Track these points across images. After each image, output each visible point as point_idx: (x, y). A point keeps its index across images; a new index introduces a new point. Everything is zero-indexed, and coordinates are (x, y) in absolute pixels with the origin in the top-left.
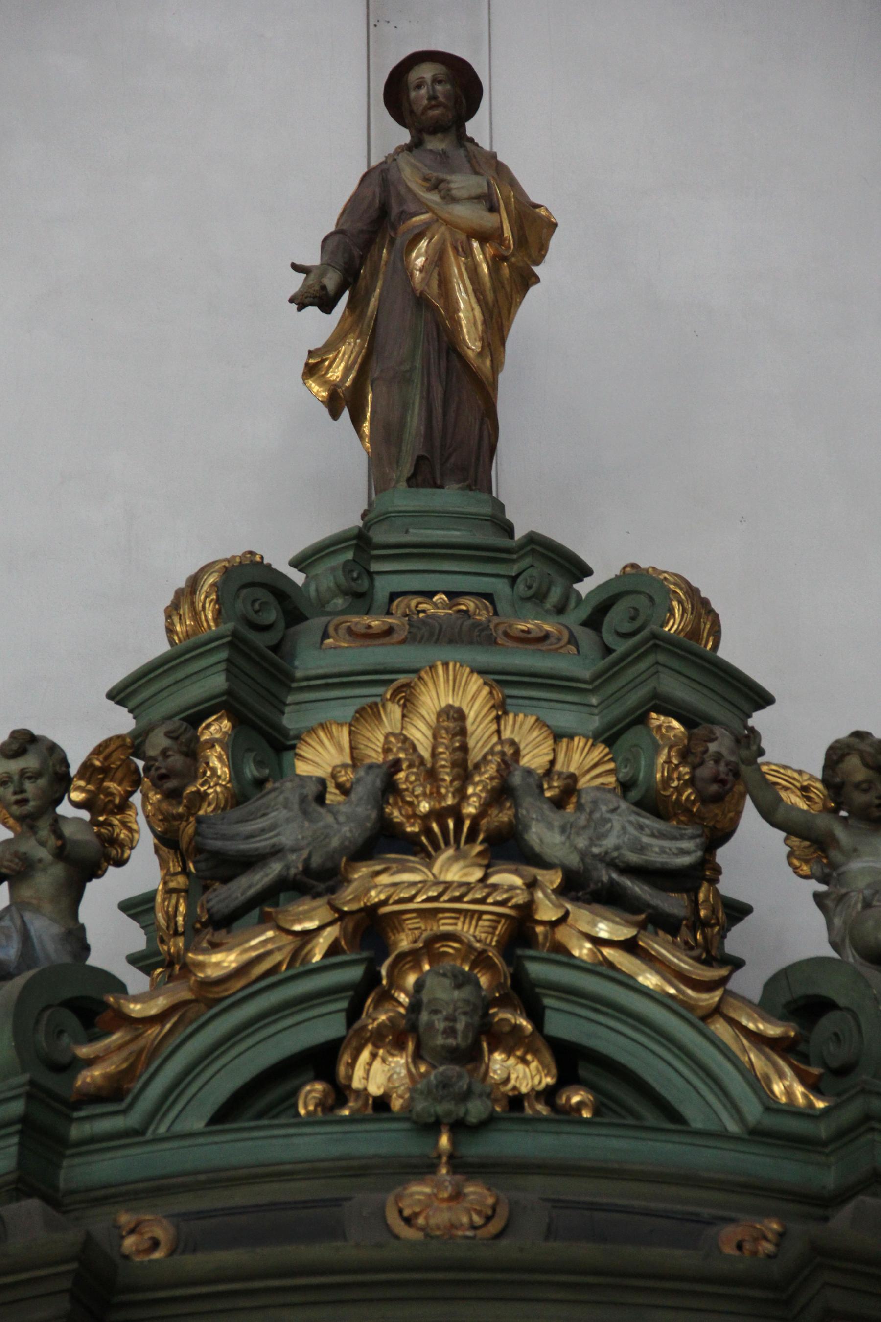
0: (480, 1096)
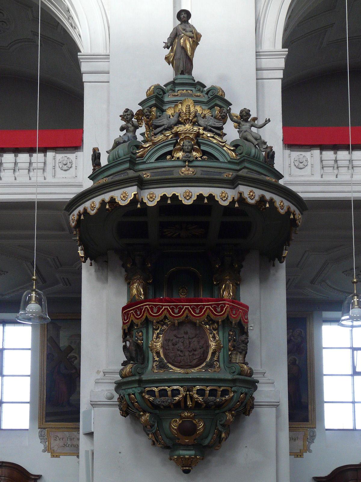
0: (192, 157)
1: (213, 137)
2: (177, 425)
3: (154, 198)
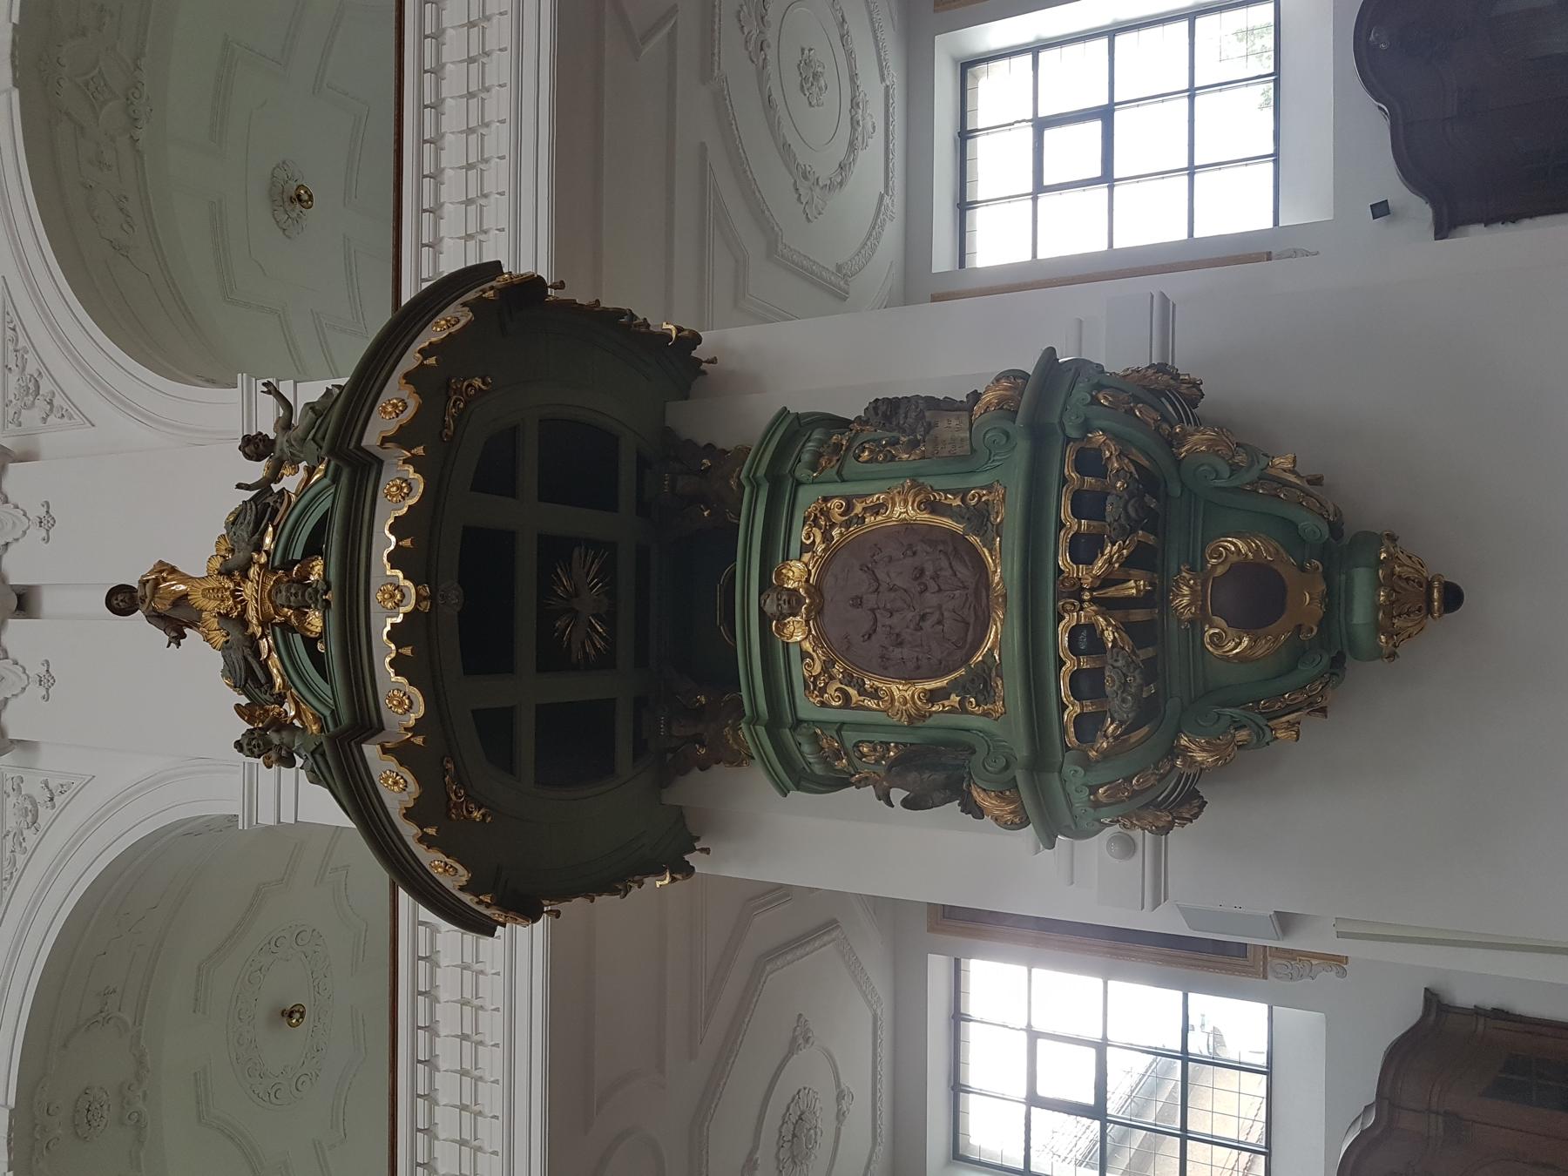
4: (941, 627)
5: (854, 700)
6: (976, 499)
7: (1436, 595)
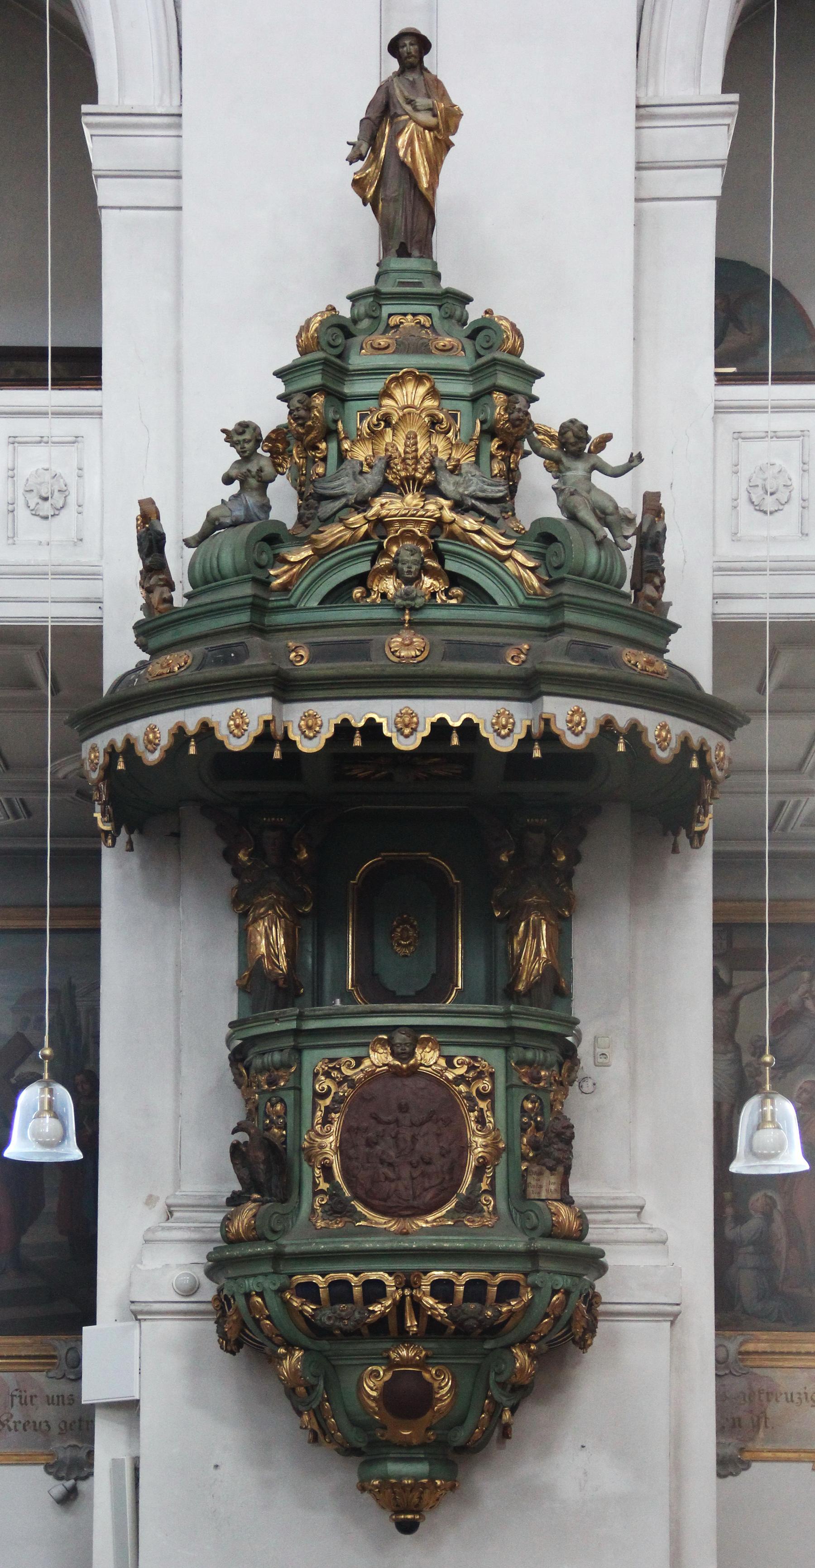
1: (479, 532)
2: (380, 1384)
3: (317, 729)
4: (383, 1180)
5: (321, 1102)
6: (485, 1202)
7: (409, 1517)
